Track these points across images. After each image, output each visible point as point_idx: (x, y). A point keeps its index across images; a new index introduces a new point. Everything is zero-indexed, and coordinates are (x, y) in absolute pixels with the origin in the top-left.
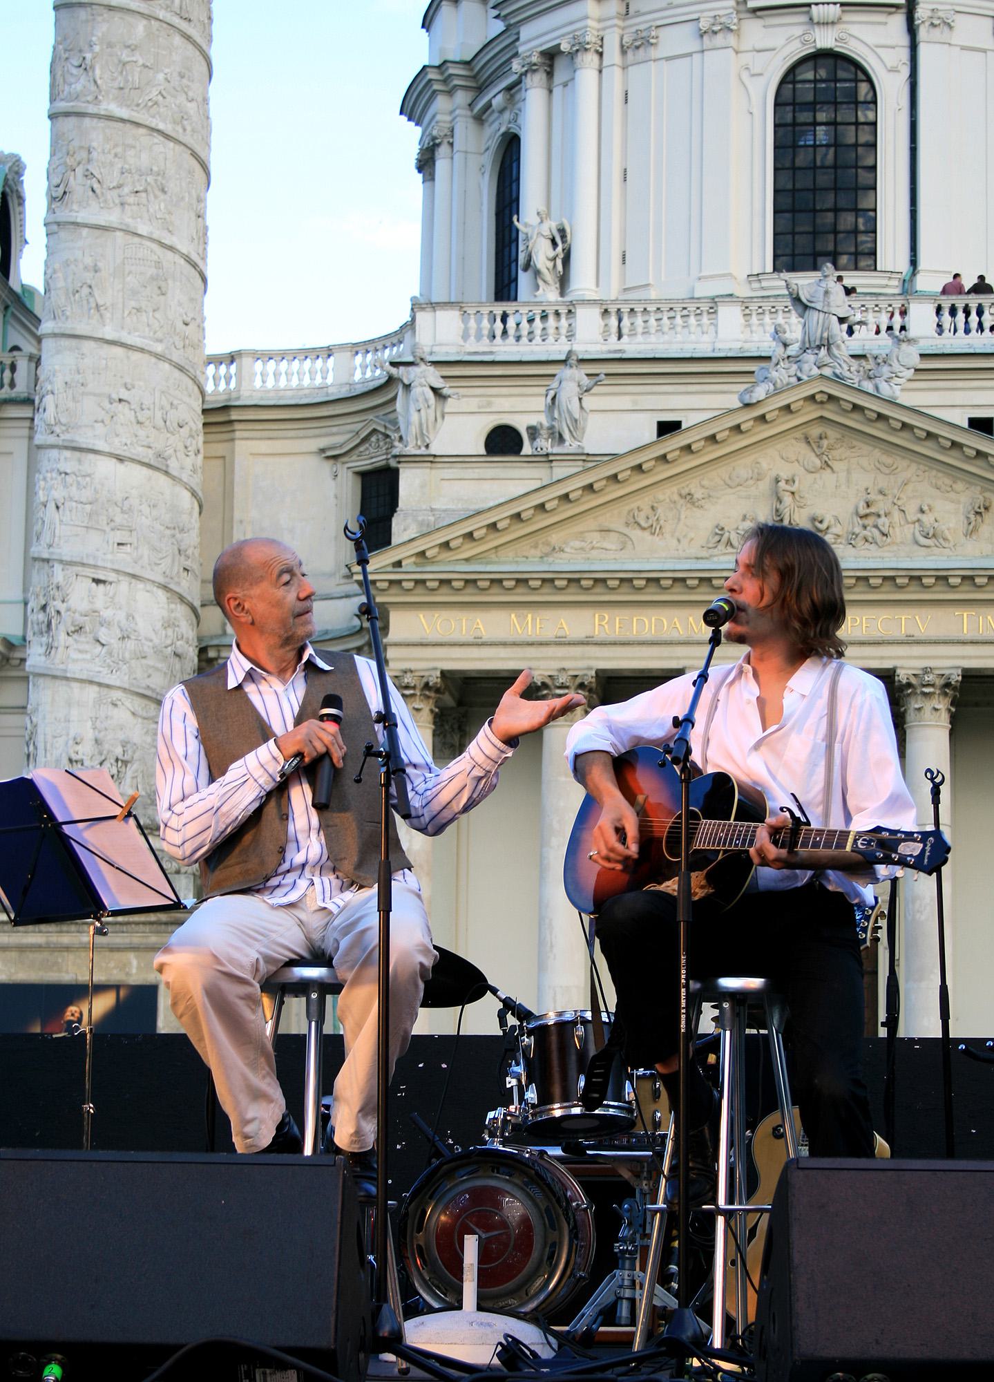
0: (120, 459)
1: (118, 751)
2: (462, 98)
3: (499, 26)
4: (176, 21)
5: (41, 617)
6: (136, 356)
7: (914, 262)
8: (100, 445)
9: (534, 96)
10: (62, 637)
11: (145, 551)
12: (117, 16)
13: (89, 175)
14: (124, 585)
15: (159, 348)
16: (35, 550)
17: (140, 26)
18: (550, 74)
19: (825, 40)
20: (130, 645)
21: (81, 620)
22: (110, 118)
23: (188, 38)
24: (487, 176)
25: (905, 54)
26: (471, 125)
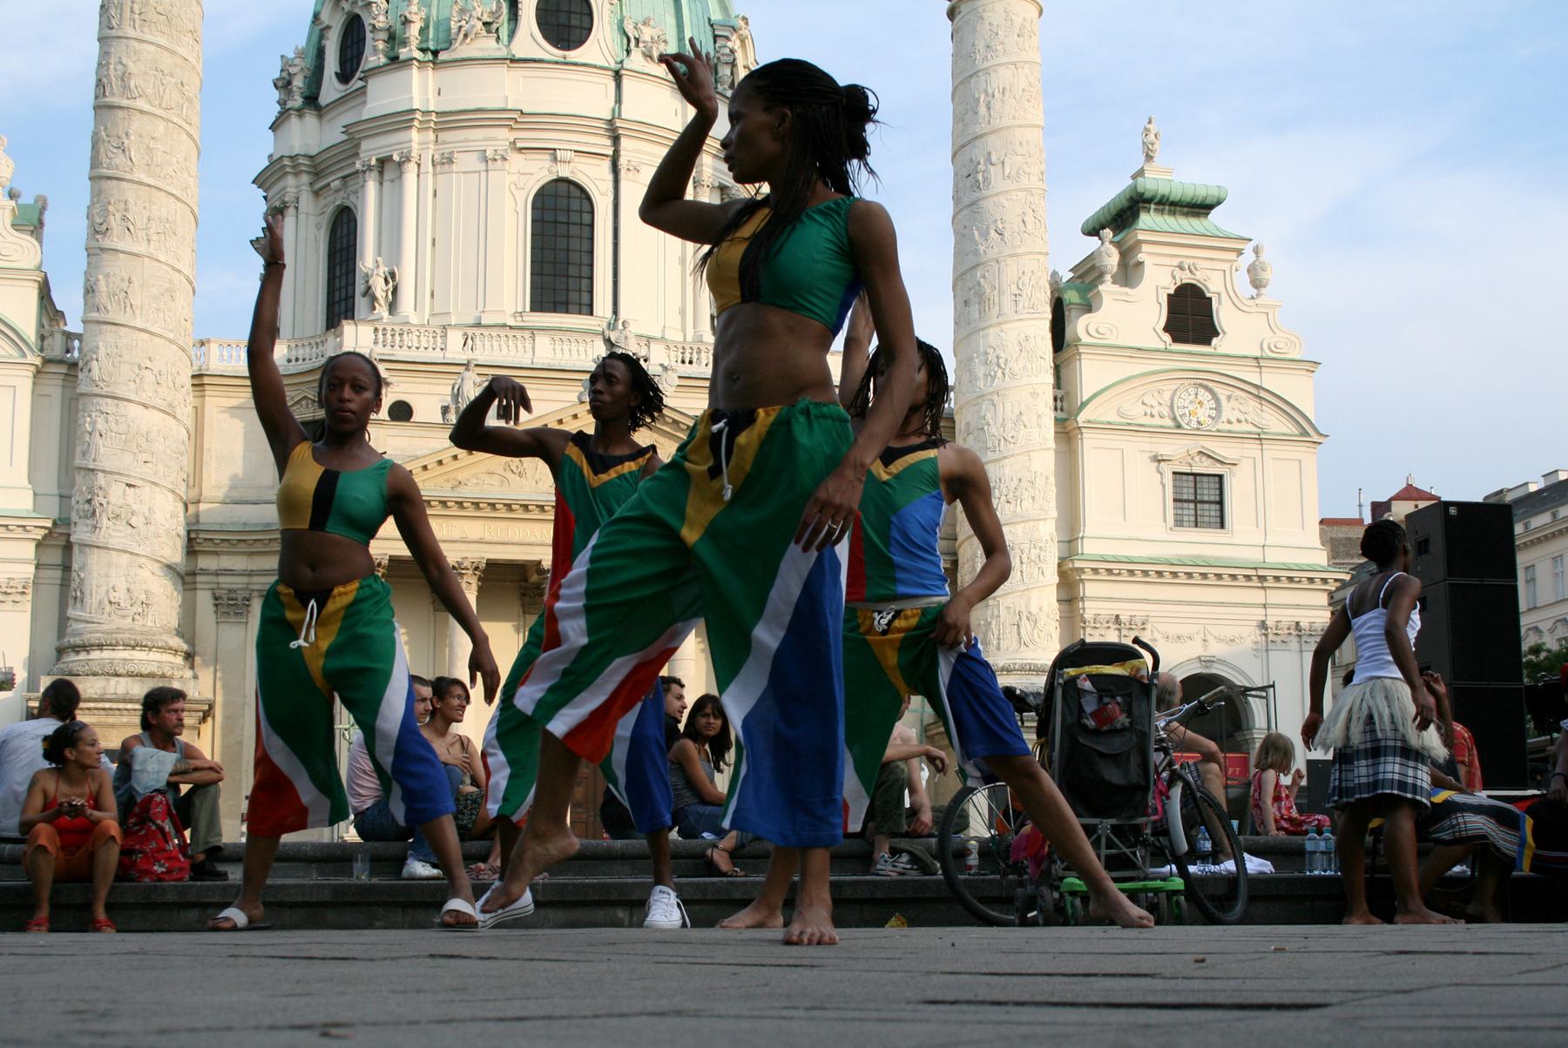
0: (145, 406)
1: (143, 597)
2: (305, 179)
3: (345, 137)
4: (184, 124)
5: (86, 507)
6: (157, 340)
7: (615, 312)
8: (133, 397)
9: (371, 187)
10: (105, 521)
11: (161, 467)
12: (146, 118)
13: (124, 219)
14: (147, 490)
15: (171, 336)
16: (78, 462)
17: (162, 126)
18: (381, 173)
19: (564, 172)
20: (152, 528)
21: (118, 511)
22: (140, 183)
23: (190, 135)
24: (323, 231)
25: (610, 185)
26: (311, 198)
